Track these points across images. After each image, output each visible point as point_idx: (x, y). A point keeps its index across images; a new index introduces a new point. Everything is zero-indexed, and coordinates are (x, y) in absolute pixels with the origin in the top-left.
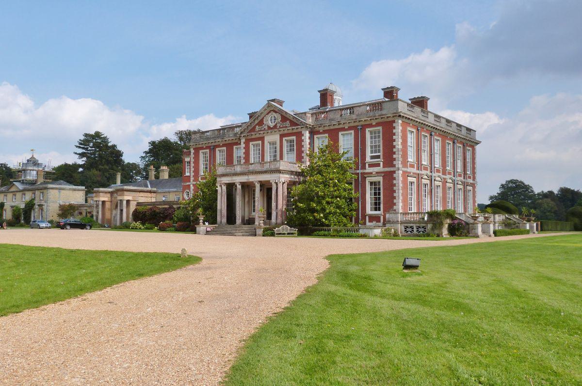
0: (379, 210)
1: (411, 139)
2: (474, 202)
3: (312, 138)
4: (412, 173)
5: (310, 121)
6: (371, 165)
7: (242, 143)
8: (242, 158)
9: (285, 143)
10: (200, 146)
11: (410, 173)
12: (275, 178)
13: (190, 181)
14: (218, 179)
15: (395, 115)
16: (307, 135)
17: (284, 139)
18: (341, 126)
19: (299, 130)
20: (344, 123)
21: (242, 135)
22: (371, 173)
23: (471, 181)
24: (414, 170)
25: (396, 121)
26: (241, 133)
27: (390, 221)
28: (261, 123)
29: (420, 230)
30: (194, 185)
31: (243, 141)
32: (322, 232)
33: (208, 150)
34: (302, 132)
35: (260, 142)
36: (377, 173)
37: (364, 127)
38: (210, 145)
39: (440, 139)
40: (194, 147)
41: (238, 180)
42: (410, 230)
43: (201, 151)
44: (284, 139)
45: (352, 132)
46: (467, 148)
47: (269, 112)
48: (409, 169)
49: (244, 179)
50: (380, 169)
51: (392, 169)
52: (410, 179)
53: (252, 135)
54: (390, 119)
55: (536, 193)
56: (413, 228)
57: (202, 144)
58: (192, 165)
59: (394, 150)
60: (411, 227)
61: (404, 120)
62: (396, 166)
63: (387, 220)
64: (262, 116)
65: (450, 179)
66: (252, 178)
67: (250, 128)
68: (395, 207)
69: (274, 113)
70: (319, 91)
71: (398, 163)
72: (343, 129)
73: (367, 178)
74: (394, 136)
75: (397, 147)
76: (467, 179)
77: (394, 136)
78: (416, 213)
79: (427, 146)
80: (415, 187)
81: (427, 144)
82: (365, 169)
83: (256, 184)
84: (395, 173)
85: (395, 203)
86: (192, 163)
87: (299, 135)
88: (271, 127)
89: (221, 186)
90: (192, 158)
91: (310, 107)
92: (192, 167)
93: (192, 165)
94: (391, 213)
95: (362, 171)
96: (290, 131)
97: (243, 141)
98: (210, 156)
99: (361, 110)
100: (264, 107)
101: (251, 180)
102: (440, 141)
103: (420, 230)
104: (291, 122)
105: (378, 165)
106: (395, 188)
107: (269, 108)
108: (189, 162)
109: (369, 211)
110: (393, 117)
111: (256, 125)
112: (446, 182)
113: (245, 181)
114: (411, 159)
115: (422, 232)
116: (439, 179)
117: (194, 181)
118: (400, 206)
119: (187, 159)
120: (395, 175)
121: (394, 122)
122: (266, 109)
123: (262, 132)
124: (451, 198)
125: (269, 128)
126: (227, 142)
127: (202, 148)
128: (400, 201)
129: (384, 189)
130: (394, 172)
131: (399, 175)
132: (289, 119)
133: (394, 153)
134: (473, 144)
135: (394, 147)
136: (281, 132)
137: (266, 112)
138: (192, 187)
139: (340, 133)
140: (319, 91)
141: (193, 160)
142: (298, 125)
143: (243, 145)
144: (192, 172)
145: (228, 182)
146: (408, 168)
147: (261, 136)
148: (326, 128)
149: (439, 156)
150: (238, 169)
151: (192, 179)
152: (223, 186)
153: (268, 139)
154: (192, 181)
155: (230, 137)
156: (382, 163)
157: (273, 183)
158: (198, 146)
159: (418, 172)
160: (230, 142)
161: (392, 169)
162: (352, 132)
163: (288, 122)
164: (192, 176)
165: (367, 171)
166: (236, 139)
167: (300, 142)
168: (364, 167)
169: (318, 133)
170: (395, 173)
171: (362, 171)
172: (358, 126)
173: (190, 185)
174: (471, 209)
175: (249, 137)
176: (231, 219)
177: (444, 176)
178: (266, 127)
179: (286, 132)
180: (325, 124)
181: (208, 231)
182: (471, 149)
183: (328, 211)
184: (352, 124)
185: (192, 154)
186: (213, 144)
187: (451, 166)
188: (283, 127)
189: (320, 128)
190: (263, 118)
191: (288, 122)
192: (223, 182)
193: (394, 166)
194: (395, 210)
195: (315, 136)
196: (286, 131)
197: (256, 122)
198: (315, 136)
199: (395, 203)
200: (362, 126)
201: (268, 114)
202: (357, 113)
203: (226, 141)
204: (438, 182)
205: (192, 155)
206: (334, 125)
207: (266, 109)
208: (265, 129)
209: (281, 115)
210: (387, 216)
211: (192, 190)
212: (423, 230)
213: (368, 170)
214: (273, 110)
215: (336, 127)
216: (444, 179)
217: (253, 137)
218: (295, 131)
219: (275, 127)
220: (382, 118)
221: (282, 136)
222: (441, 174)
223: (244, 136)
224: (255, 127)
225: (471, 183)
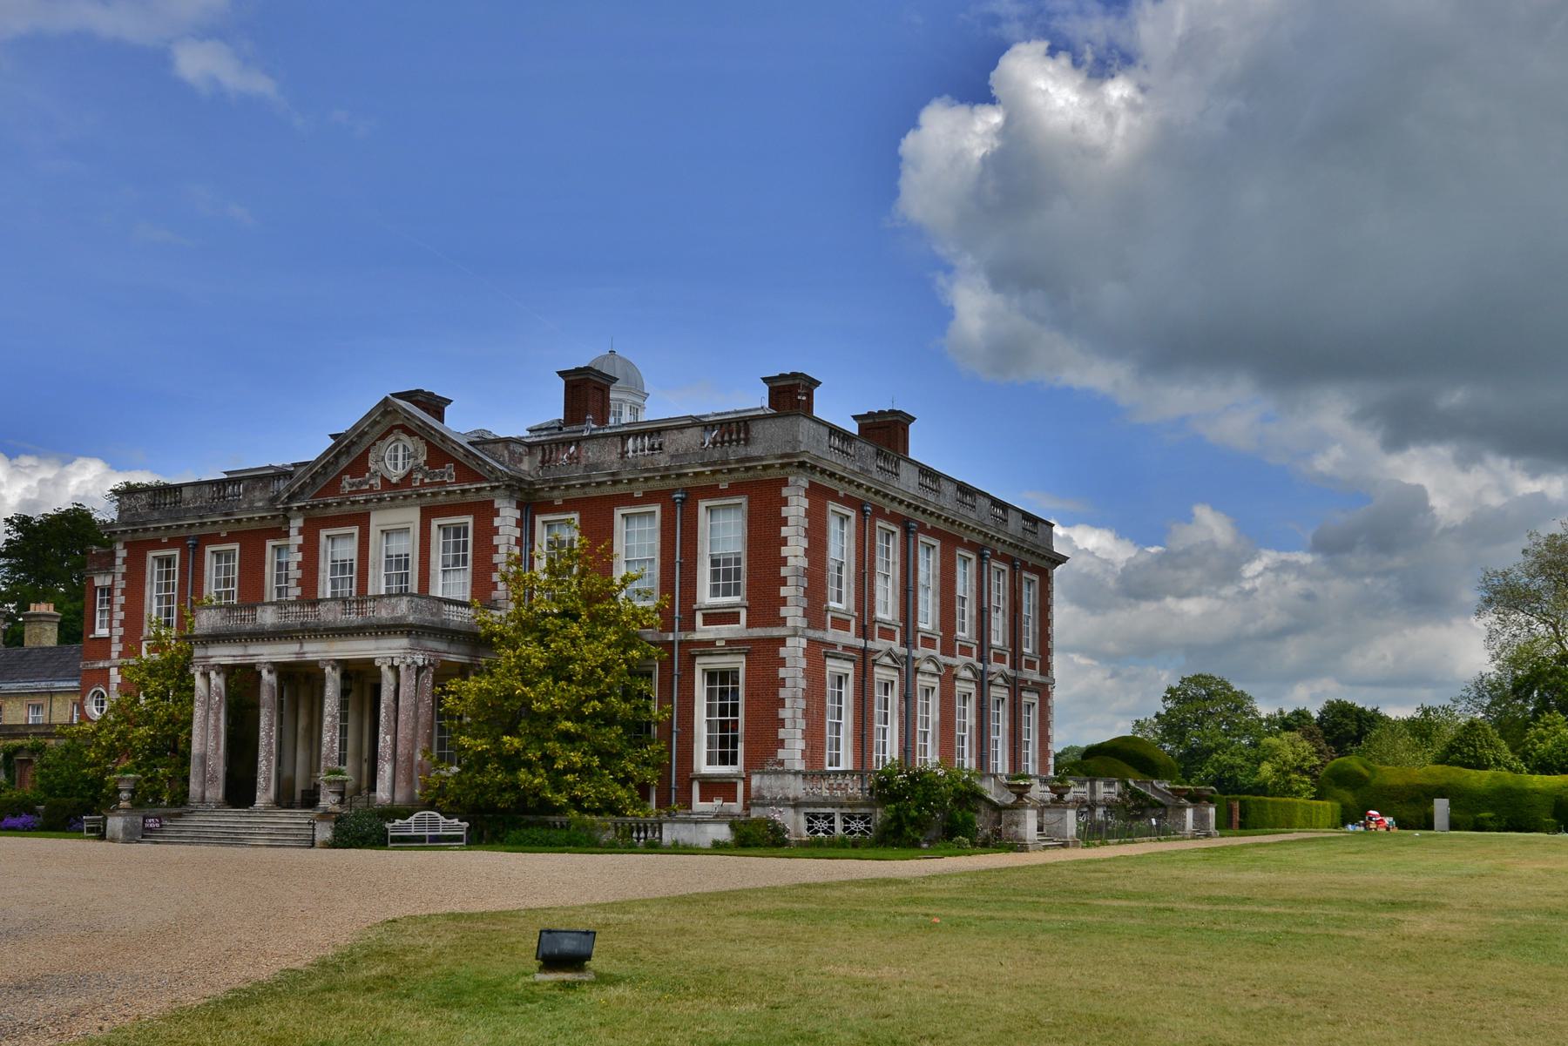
0: (734, 762)
1: (840, 544)
2: (1044, 739)
4: (840, 648)
6: (713, 618)
7: (294, 532)
8: (293, 583)
9: (436, 537)
10: (150, 536)
11: (834, 646)
12: (392, 653)
13: (108, 657)
14: (198, 652)
15: (786, 460)
17: (435, 523)
18: (621, 489)
19: (486, 496)
20: (630, 481)
21: (295, 505)
22: (711, 643)
23: (1034, 675)
24: (849, 638)
25: (791, 479)
26: (291, 498)
28: (359, 466)
29: (853, 825)
31: (297, 523)
32: (536, 833)
33: (176, 552)
34: (493, 502)
35: (355, 530)
36: (729, 642)
37: (692, 497)
38: (183, 532)
39: (937, 543)
40: (128, 538)
41: (267, 654)
42: (825, 825)
43: (151, 554)
44: (435, 523)
45: (657, 509)
46: (1025, 574)
47: (389, 432)
48: (831, 635)
49: (285, 652)
51: (776, 632)
52: (833, 666)
53: (327, 505)
54: (773, 474)
55: (1264, 716)
56: (833, 822)
57: (157, 529)
58: (119, 599)
59: (784, 572)
60: (828, 817)
61: (817, 478)
62: (790, 623)
63: (753, 794)
64: (366, 441)
65: (968, 666)
66: (315, 651)
67: (322, 483)
68: (781, 754)
69: (404, 437)
70: (561, 374)
71: (793, 614)
72: (628, 500)
73: (699, 660)
74: (783, 528)
75: (791, 561)
76: (1021, 670)
77: (783, 528)
78: (852, 773)
79: (894, 563)
80: (848, 691)
81: (895, 556)
82: (694, 629)
83: (328, 669)
84: (784, 646)
85: (783, 741)
86: (117, 592)
87: (485, 513)
88: (394, 480)
90: (119, 577)
91: (535, 423)
92: (117, 608)
93: (119, 599)
94: (767, 773)
95: (682, 636)
96: (457, 499)
97: (297, 523)
98: (183, 572)
99: (686, 440)
100: (369, 415)
101: (310, 657)
102: (938, 549)
103: (853, 825)
104: (459, 465)
105: (733, 618)
106: (783, 693)
107: (389, 418)
108: (109, 590)
109: (702, 766)
110: (783, 466)
111: (345, 472)
112: (955, 677)
114: (841, 603)
115: (861, 832)
116: (931, 667)
117: (121, 655)
118: (793, 751)
119: (100, 581)
120: (783, 652)
121: (785, 483)
122: (376, 423)
123: (361, 498)
124: (971, 727)
125: (386, 482)
126: (244, 526)
127: (156, 544)
128: (799, 734)
129: (749, 695)
130: (781, 641)
131: (794, 650)
132: (450, 459)
134: (1043, 564)
135: (784, 561)
136: (427, 501)
137: (378, 430)
138: (115, 677)
139: (618, 513)
140: (561, 374)
141: (121, 584)
142: (481, 479)
143: (296, 539)
144: (116, 623)
145: (229, 661)
146: (825, 629)
147: (357, 509)
148: (575, 494)
149: (934, 595)
150: (268, 617)
151: (116, 648)
152: (213, 674)
153: (378, 520)
154: (114, 655)
155: (254, 507)
156: (743, 614)
157: (384, 668)
158: (141, 536)
159: (860, 643)
160: (254, 526)
162: (657, 509)
163: (450, 468)
164: (116, 639)
165: (697, 636)
166: (274, 517)
167: (486, 533)
168: (692, 627)
169: (548, 507)
170: (784, 646)
171: (682, 636)
172: (674, 491)
173: (106, 670)
174: (1034, 761)
175: (317, 513)
176: (239, 791)
177: (949, 660)
178: (376, 482)
179: (441, 499)
180: (569, 479)
181: (151, 830)
182: (1036, 578)
183: (560, 765)
184: (656, 485)
185: (119, 561)
186: (196, 532)
187: (970, 629)
188: (431, 485)
189: (556, 493)
190: (367, 451)
191: (450, 468)
192: (213, 661)
193: (782, 622)
194: (781, 763)
195: (539, 519)
196: (440, 498)
197: (344, 462)
198: (539, 519)
199: (783, 741)
200: (686, 490)
201: (383, 437)
202: (672, 450)
203: (239, 521)
204: (927, 678)
205: (120, 567)
206: (599, 484)
207: (376, 423)
208: (371, 486)
209: (428, 443)
210: (755, 781)
211: (113, 687)
212: (862, 826)
213: (703, 632)
215: (608, 491)
216: (949, 667)
217: (332, 511)
218: (470, 498)
219: (407, 480)
220: (748, 469)
221: (428, 514)
222: (936, 652)
223: (299, 508)
224: (338, 479)
225: (1033, 683)
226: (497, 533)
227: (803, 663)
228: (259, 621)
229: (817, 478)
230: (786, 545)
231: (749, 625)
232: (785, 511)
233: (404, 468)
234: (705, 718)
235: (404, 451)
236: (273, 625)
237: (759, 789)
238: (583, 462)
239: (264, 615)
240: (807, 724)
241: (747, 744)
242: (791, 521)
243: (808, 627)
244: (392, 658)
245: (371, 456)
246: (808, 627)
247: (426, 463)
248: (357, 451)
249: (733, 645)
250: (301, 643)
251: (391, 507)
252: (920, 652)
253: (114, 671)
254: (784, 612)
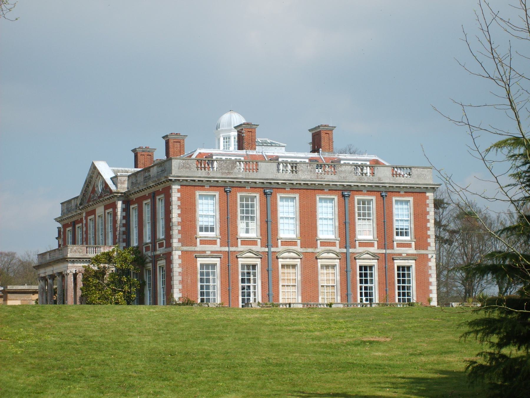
3: (126, 210)
5: (126, 185)
11: (204, 252)
16: (120, 204)
35: (93, 216)
48: (199, 247)
54: (167, 184)
71: (175, 242)
73: (159, 262)
113: (51, 273)
131: (176, 255)
159: (226, 249)
161: (168, 250)
165: (158, 253)
168: (154, 249)
177: (310, 250)
227: (180, 261)
229: (185, 183)
231: (166, 248)
234: (162, 286)
236: (49, 260)
240: (183, 287)
243: (182, 246)
246: (182, 246)
248: (93, 183)
252: (281, 248)
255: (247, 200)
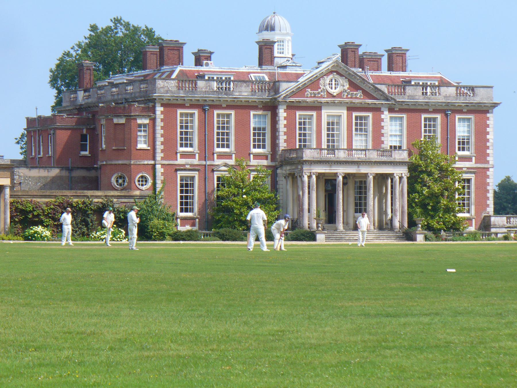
17: (355, 114)
27: (495, 225)
30: (163, 165)
35: (314, 113)
50: (472, 164)
69: (337, 77)
77: (487, 128)
84: (489, 171)
89: (310, 177)
117: (162, 159)
120: (488, 173)
130: (488, 169)
133: (488, 148)
170: (489, 171)
193: (488, 162)
202: (444, 94)
208: (322, 95)
209: (349, 81)
213: (459, 165)
214: (335, 72)
226: (383, 121)
228: (336, 155)
230: (488, 134)
231: (476, 163)
232: (488, 122)
233: (335, 89)
235: (335, 81)
237: (494, 222)
238: (407, 94)
239: (339, 154)
241: (476, 206)
242: (490, 126)
244: (402, 174)
245: (322, 82)
247: (348, 89)
249: (469, 171)
250: (358, 167)
251: (333, 106)
253: (158, 167)
254: (488, 159)
255: (430, 121)
